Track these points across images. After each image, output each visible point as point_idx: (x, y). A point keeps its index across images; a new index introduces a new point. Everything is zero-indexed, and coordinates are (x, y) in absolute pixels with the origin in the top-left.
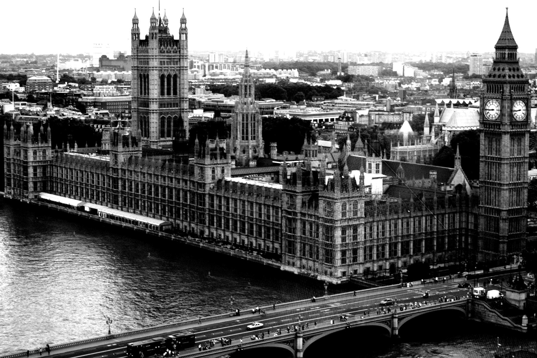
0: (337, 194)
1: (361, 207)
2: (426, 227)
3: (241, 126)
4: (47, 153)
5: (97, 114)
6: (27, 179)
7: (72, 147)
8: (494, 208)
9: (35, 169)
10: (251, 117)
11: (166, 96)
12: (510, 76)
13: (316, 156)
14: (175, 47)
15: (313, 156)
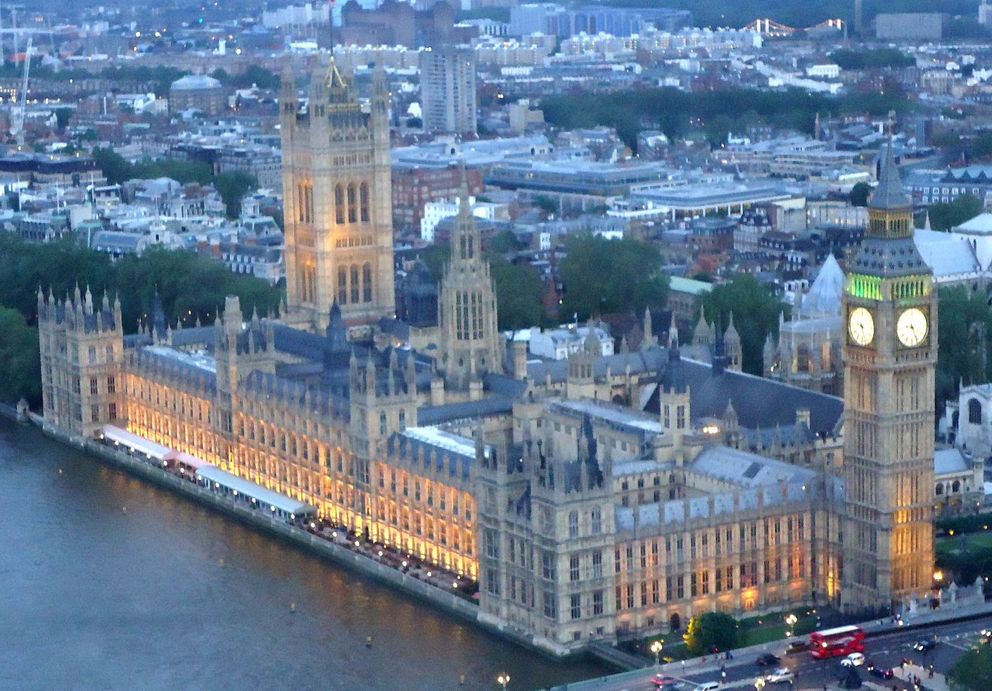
0: (559, 495)
1: (608, 517)
2: (742, 542)
3: (455, 314)
4: (115, 349)
5: (248, 226)
6: (80, 399)
7: (163, 335)
8: (868, 509)
9: (94, 382)
10: (473, 297)
11: (347, 224)
12: (892, 267)
13: (589, 375)
14: (363, 128)
15: (583, 376)
